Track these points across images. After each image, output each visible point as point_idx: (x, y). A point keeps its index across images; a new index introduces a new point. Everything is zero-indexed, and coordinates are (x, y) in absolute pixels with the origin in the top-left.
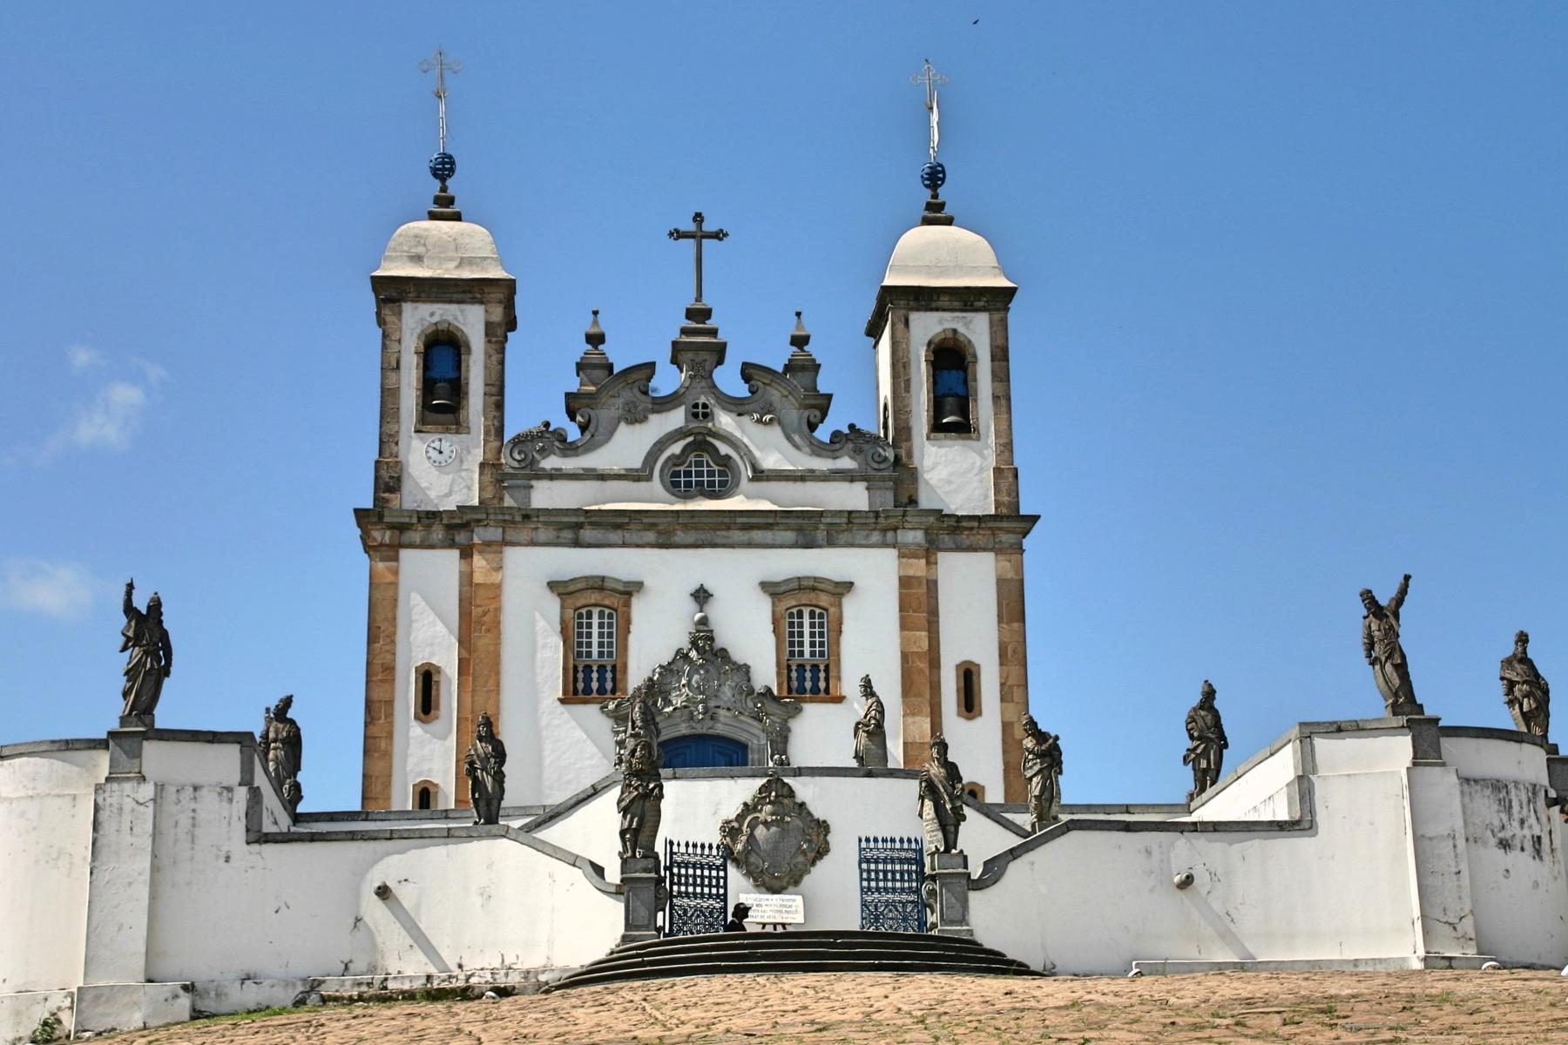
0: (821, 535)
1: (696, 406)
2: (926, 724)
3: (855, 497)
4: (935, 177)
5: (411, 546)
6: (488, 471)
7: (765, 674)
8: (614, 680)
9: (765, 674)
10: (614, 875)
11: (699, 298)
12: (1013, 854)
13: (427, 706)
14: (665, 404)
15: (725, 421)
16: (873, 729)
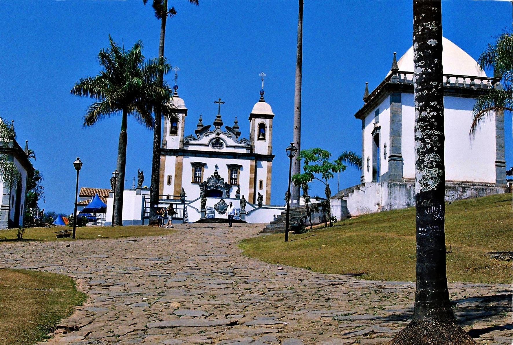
0: (237, 157)
1: (217, 133)
2: (253, 190)
3: (244, 151)
4: (262, 93)
5: (168, 155)
6: (181, 142)
7: (227, 180)
8: (201, 179)
9: (227, 180)
10: (200, 210)
11: (219, 114)
12: (253, 210)
13: (169, 182)
14: (212, 133)
15: (222, 136)
16: (238, 192)
